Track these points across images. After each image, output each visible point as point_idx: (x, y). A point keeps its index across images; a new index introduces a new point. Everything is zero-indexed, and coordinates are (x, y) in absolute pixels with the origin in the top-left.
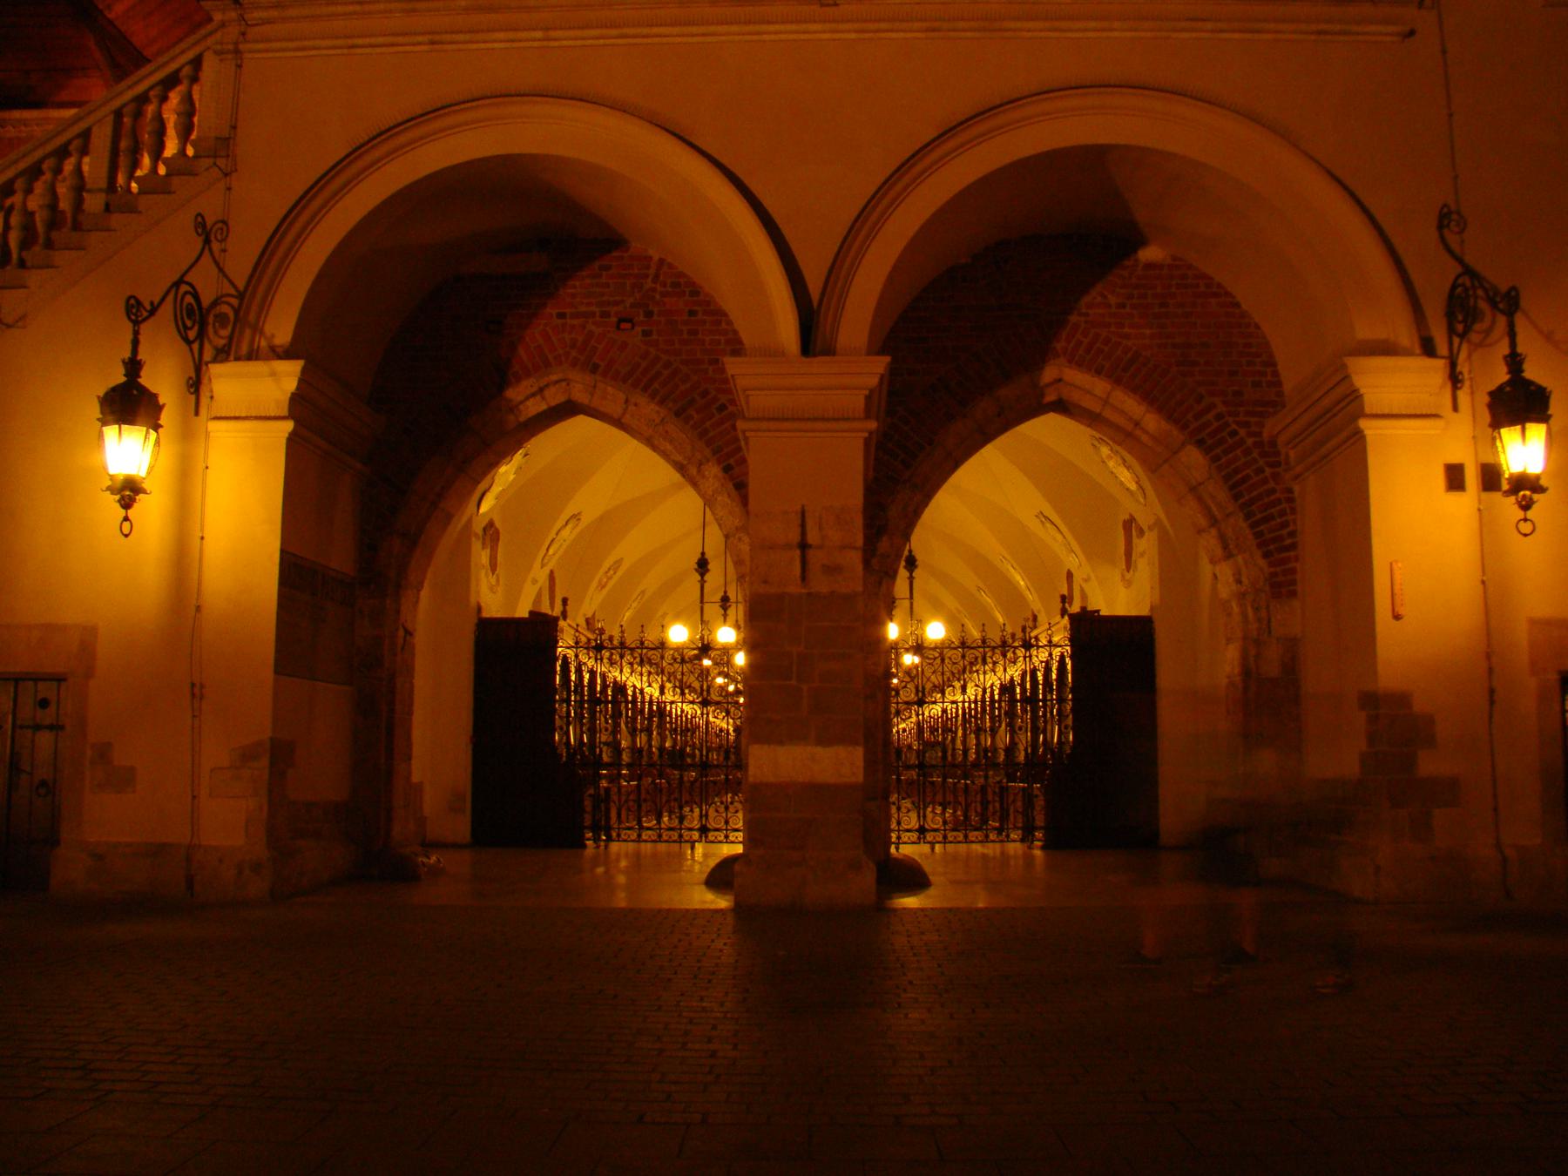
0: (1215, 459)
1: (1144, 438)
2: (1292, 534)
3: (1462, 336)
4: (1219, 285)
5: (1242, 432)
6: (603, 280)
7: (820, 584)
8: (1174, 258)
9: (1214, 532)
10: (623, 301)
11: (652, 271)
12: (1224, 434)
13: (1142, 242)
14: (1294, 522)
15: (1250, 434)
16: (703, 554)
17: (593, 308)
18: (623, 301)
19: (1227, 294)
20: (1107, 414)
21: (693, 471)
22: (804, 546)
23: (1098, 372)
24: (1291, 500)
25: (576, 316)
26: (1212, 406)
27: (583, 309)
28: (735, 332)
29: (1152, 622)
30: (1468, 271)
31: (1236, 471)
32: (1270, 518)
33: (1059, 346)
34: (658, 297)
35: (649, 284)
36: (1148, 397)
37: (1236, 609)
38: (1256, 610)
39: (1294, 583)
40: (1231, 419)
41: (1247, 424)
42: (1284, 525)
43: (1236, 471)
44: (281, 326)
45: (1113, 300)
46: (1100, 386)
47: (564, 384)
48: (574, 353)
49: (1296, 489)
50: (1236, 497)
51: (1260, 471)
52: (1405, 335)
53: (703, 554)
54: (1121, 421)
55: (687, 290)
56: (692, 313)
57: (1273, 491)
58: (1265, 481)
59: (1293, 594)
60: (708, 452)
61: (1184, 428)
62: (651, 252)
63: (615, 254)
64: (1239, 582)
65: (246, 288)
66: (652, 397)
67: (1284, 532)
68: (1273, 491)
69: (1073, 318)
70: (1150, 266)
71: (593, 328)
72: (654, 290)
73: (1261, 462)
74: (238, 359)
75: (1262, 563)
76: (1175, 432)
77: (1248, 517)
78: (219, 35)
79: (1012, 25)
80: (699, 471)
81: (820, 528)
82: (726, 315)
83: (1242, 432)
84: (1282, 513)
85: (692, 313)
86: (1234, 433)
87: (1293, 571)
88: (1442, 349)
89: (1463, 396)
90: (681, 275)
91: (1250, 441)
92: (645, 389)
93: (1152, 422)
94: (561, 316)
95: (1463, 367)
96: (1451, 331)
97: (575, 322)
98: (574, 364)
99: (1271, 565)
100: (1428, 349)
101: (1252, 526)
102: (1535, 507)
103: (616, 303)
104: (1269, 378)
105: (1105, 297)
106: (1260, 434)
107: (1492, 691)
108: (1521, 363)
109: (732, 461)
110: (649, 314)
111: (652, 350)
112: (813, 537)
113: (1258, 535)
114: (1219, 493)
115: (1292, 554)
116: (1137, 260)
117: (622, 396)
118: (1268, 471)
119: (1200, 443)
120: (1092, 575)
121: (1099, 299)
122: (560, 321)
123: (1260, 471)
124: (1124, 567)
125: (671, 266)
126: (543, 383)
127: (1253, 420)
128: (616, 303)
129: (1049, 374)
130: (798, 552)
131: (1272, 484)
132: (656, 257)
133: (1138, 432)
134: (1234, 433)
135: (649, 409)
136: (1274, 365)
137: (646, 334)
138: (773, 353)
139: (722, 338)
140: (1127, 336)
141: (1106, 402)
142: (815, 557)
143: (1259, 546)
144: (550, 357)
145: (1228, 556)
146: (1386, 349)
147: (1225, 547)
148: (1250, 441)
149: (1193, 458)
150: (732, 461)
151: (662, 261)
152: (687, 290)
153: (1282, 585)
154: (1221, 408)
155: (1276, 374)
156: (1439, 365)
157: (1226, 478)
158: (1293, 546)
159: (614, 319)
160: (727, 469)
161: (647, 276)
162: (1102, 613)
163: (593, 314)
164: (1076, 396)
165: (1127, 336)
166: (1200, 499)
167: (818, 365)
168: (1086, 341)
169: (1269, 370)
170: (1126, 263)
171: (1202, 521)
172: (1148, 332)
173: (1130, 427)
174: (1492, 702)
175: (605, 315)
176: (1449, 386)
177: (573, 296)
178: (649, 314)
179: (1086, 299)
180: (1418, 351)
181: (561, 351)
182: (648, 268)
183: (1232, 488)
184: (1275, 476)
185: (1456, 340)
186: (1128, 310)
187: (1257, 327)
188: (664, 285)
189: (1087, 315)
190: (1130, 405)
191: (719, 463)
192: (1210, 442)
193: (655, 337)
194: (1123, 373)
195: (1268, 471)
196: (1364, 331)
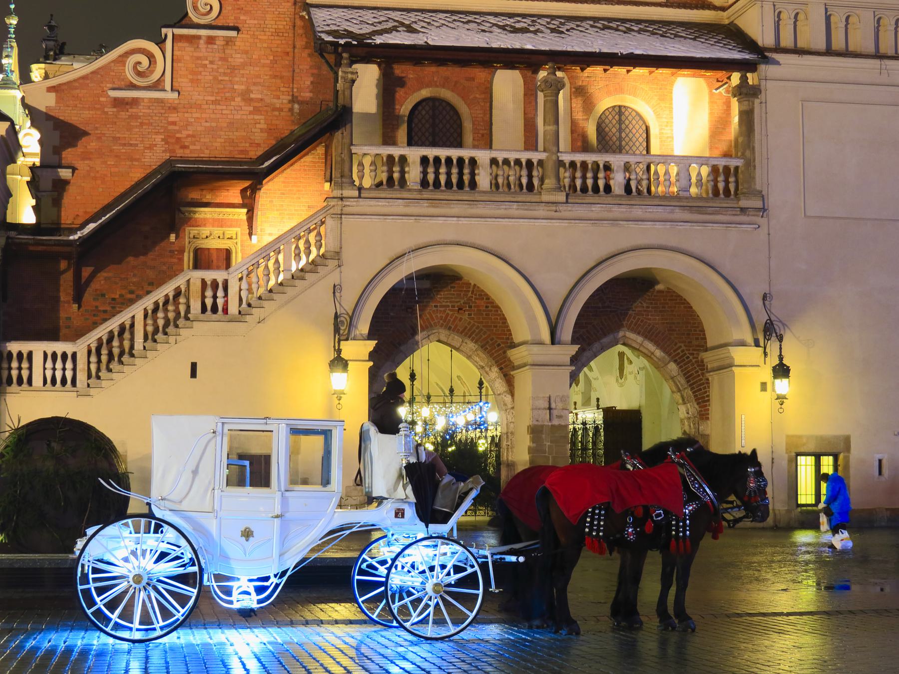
0: (681, 367)
1: (655, 359)
2: (708, 396)
3: (768, 340)
4: (685, 300)
5: (691, 357)
6: (452, 292)
7: (556, 422)
8: (668, 288)
9: (679, 394)
10: (460, 301)
11: (471, 289)
12: (685, 358)
13: (658, 283)
14: (709, 391)
15: (694, 358)
16: (451, 386)
17: (449, 304)
18: (460, 301)
19: (688, 303)
20: (641, 349)
21: (487, 369)
22: (550, 409)
23: (639, 334)
24: (708, 383)
25: (441, 306)
26: (680, 347)
27: (444, 304)
28: (504, 315)
29: (641, 413)
30: (770, 319)
31: (688, 372)
32: (700, 390)
33: (625, 323)
34: (473, 300)
35: (470, 294)
36: (657, 344)
37: (686, 423)
38: (694, 424)
39: (708, 414)
40: (687, 352)
41: (692, 354)
42: (706, 392)
43: (688, 372)
44: (364, 327)
45: (645, 305)
46: (640, 339)
47: (437, 334)
48: (441, 322)
49: (710, 379)
50: (688, 382)
51: (697, 372)
52: (750, 339)
53: (451, 386)
54: (646, 352)
55: (485, 298)
56: (487, 307)
57: (702, 380)
58: (699, 376)
59: (708, 419)
60: (493, 362)
61: (670, 355)
62: (471, 282)
63: (457, 282)
64: (688, 413)
65: (353, 313)
66: (472, 340)
67: (705, 395)
68: (702, 380)
69: (630, 312)
70: (660, 292)
71: (449, 312)
72: (472, 297)
73: (698, 368)
74: (351, 340)
75: (697, 406)
76: (666, 357)
77: (692, 389)
78: (332, 209)
79: (621, 222)
80: (490, 369)
81: (555, 403)
82: (500, 308)
83: (691, 357)
84: (705, 388)
85: (487, 307)
86: (688, 357)
87: (708, 410)
88: (762, 344)
89: (768, 359)
90: (483, 291)
91: (694, 361)
92: (469, 337)
93: (658, 353)
94: (436, 306)
95: (768, 350)
96: (765, 337)
97: (442, 309)
98: (441, 326)
99: (700, 407)
100: (757, 344)
101: (694, 393)
102: (784, 404)
103: (457, 302)
104: (702, 336)
105: (642, 303)
106: (698, 358)
107: (773, 459)
108: (782, 358)
109: (503, 366)
110: (470, 307)
111: (471, 321)
112: (553, 406)
113: (695, 396)
114: (682, 380)
115: (708, 403)
116: (654, 289)
117: (461, 340)
118: (700, 372)
119: (675, 361)
120: (600, 378)
121: (640, 304)
122: (435, 309)
123: (697, 372)
124: (618, 375)
125: (478, 287)
126: (429, 333)
127: (695, 352)
128: (457, 302)
129: (621, 334)
130: (548, 411)
131: (701, 377)
132: (472, 284)
133: (652, 356)
134: (688, 357)
135: (471, 345)
136: (704, 331)
137: (470, 315)
138: (541, 343)
139: (499, 318)
140: (649, 319)
141: (641, 345)
142: (555, 413)
143: (696, 400)
144: (432, 323)
145: (684, 403)
146: (742, 344)
147: (683, 400)
148: (694, 361)
149: (672, 366)
150: (503, 366)
151: (475, 285)
152: (485, 298)
153: (703, 415)
154: (685, 348)
155: (704, 334)
156: (761, 350)
157: (684, 375)
158: (708, 401)
159: (457, 309)
160: (501, 369)
161: (469, 291)
162: (617, 408)
163: (449, 306)
164: (630, 342)
165: (649, 319)
166: (675, 382)
167: (556, 348)
168: (634, 321)
169: (702, 333)
170: (651, 290)
171: (675, 389)
172: (657, 318)
173: (649, 354)
174: (773, 463)
175: (453, 306)
176: (763, 355)
177: (441, 298)
178: (470, 307)
179: (635, 304)
180: (753, 344)
181: (436, 321)
182: (470, 288)
183: (686, 378)
184: (703, 374)
185: (766, 341)
186: (650, 309)
187: (698, 316)
188: (476, 295)
189: (635, 311)
190: (650, 346)
191: (498, 366)
192: (679, 361)
193: (473, 316)
194: (649, 335)
195: (700, 372)
196: (736, 336)
